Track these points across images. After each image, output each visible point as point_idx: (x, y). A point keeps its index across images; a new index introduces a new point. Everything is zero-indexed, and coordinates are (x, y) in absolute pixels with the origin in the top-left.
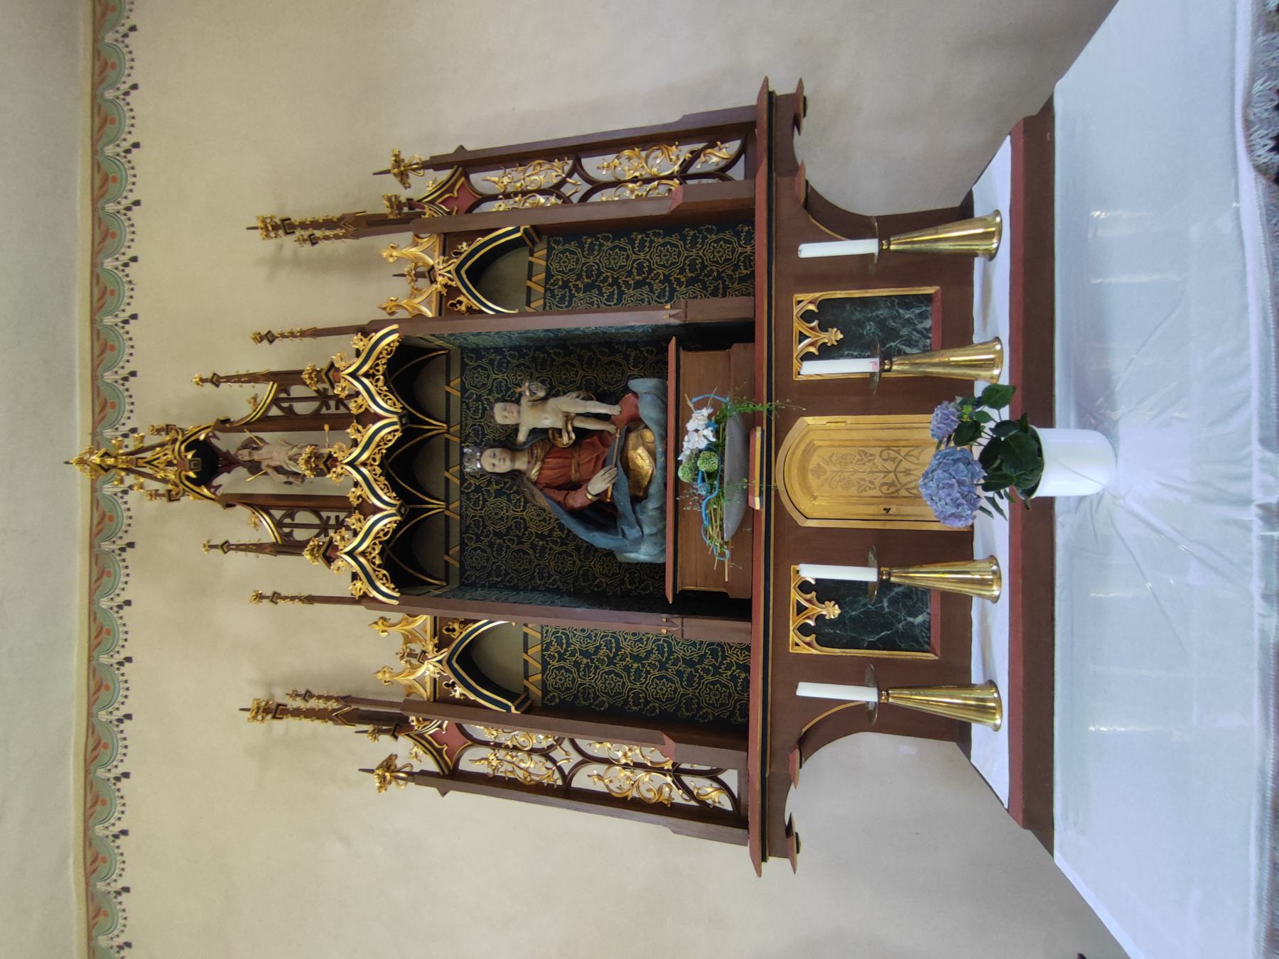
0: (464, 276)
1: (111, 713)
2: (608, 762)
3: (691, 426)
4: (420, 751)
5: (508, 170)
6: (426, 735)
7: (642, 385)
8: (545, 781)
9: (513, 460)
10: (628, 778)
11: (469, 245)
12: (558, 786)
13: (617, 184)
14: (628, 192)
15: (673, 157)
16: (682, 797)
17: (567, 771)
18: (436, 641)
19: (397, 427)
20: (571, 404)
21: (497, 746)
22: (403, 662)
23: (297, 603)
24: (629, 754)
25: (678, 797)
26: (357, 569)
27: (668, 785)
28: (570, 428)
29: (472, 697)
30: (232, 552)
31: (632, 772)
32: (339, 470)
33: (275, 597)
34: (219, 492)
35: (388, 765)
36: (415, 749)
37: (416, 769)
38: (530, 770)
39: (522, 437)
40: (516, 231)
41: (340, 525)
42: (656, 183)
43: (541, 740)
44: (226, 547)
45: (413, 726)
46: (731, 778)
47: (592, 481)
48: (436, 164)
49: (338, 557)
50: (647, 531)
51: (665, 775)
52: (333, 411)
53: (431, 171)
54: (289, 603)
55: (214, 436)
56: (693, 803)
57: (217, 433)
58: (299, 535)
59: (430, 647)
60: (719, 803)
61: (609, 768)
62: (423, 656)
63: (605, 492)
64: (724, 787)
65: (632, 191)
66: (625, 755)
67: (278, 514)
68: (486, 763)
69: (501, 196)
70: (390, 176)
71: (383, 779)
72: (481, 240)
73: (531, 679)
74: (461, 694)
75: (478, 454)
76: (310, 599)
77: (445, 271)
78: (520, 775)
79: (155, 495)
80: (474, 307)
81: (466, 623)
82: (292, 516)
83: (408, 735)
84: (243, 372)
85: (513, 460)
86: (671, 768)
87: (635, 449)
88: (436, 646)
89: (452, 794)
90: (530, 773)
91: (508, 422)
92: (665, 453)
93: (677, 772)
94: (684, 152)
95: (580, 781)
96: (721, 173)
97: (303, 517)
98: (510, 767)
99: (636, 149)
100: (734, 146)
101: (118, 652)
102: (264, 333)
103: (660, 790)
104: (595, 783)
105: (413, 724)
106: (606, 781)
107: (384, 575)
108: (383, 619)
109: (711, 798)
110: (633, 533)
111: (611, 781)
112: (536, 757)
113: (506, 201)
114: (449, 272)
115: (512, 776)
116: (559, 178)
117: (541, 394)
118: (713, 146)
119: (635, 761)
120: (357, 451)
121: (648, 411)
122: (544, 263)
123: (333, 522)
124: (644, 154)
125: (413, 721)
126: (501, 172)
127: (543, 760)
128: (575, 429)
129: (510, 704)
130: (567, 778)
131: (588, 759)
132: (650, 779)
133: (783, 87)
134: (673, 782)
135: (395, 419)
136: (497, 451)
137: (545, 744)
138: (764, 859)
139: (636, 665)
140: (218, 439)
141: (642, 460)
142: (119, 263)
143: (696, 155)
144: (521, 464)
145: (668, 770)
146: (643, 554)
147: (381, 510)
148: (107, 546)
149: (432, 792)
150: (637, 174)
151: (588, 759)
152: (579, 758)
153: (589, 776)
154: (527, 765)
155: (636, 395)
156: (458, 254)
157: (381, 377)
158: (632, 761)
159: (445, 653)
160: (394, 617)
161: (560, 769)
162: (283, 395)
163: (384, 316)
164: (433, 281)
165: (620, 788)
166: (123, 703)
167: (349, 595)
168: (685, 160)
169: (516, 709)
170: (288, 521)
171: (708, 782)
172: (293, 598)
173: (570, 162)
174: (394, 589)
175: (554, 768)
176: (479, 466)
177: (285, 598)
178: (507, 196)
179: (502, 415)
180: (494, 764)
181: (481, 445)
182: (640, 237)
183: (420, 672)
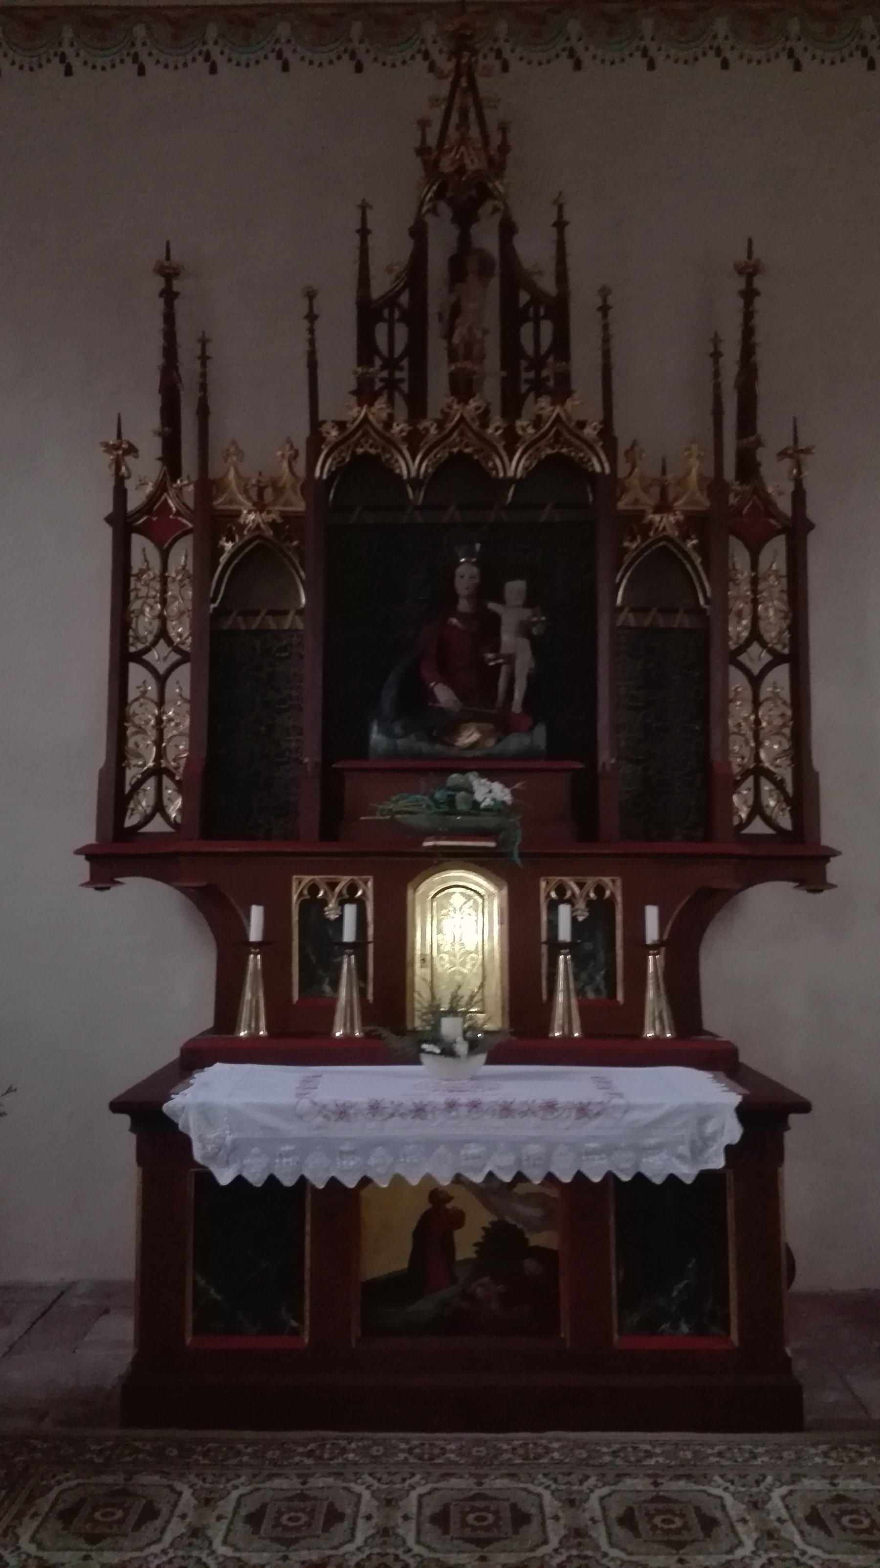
0: (661, 544)
1: (144, 44)
2: (161, 703)
3: (497, 787)
4: (149, 489)
5: (784, 581)
6: (165, 495)
7: (540, 737)
8: (131, 633)
9: (468, 597)
10: (147, 722)
11: (694, 546)
12: (127, 649)
13: (756, 704)
14: (746, 715)
15: (778, 761)
16: (134, 777)
17: (146, 657)
18: (279, 520)
19: (501, 475)
20: (525, 662)
21: (164, 580)
22: (254, 482)
23: (305, 347)
24: (173, 724)
25: (132, 775)
26: (351, 427)
27: (144, 765)
28: (501, 661)
29: (223, 560)
30: (356, 240)
31: (153, 727)
32: (455, 407)
33: (311, 317)
34: (430, 219)
35: (132, 450)
36: (151, 484)
37: (129, 484)
38: (141, 616)
39: (492, 606)
40: (707, 601)
41: (391, 385)
42: (753, 744)
43: (180, 630)
44: (364, 232)
45: (175, 482)
46: (157, 825)
47: (446, 687)
48: (799, 496)
49: (360, 405)
50: (400, 742)
51: (155, 761)
52: (525, 375)
53: (790, 487)
54: (306, 336)
55: (496, 210)
56: (128, 788)
57: (498, 217)
58: (381, 332)
59: (272, 516)
60: (132, 814)
61: (156, 703)
62: (260, 506)
63: (436, 701)
64: (148, 819)
65: (746, 719)
66: (171, 720)
67: (404, 299)
68: (144, 567)
69: (753, 574)
70: (790, 443)
71: (116, 447)
72: (698, 561)
73: (240, 618)
74: (223, 548)
75: (474, 560)
76: (313, 366)
77: (666, 522)
78: (135, 606)
79: (424, 124)
80: (627, 556)
81: (298, 550)
82: (400, 320)
83: (164, 475)
84: (570, 262)
85: (468, 597)
86: (163, 766)
87: (479, 730)
88: (274, 521)
89: (107, 532)
90: (137, 617)
91: (507, 595)
92: (475, 759)
93: (158, 772)
94: (786, 773)
95: (136, 673)
96: (757, 809)
97: (402, 333)
98: (143, 591)
99: (791, 723)
100: (786, 822)
101: (222, 53)
102: (611, 300)
103: (139, 756)
104: (138, 687)
105: (179, 482)
106: (142, 700)
107: (344, 459)
108: (296, 455)
109: (136, 806)
110: (398, 730)
111: (141, 705)
112: (156, 624)
113: (748, 580)
114: (664, 529)
115: (133, 595)
116: (768, 640)
117: (534, 631)
118: (787, 800)
119: (165, 730)
120: (476, 425)
121: (515, 742)
122: (676, 626)
123: (398, 375)
124: (787, 731)
125: (181, 481)
126: (784, 572)
127: (155, 631)
128: (498, 666)
129: (218, 601)
130: (138, 658)
131: (161, 680)
132: (148, 745)
133: (834, 870)
134: (148, 769)
135: (510, 473)
136: (477, 581)
137: (172, 634)
138: (89, 857)
139: (263, 729)
140: (493, 213)
141: (469, 736)
142: (720, 41)
143: (779, 785)
144: (463, 605)
145: (160, 764)
146: (376, 737)
147: (414, 459)
148: (356, 29)
149: (109, 509)
150: (764, 724)
151: (161, 680)
152: (162, 668)
153: (144, 682)
154: (148, 615)
155: (531, 729)
156: (686, 537)
157: (555, 451)
158: (165, 727)
159: (269, 533)
160: (301, 466)
161: (147, 650)
162: (542, 311)
163: (623, 446)
164: (658, 510)
165: (135, 714)
166: (158, 62)
167: (321, 417)
168: (774, 774)
169: (215, 609)
170: (397, 315)
171: (152, 802)
172: (312, 342)
173: (786, 651)
174: (329, 470)
175: (148, 644)
176: (463, 560)
177: (311, 331)
178: (754, 582)
179: (515, 588)
180: (145, 576)
181: (484, 564)
182: (698, 728)
183: (240, 497)
